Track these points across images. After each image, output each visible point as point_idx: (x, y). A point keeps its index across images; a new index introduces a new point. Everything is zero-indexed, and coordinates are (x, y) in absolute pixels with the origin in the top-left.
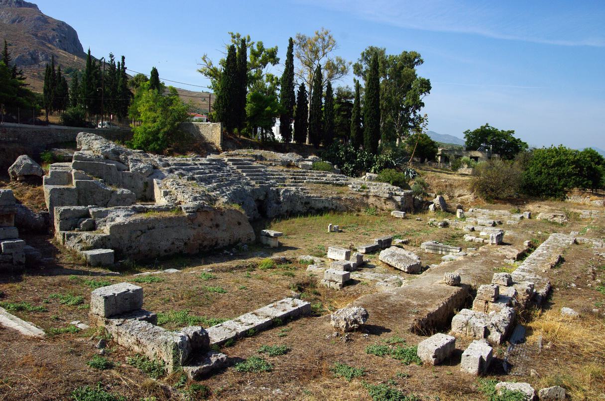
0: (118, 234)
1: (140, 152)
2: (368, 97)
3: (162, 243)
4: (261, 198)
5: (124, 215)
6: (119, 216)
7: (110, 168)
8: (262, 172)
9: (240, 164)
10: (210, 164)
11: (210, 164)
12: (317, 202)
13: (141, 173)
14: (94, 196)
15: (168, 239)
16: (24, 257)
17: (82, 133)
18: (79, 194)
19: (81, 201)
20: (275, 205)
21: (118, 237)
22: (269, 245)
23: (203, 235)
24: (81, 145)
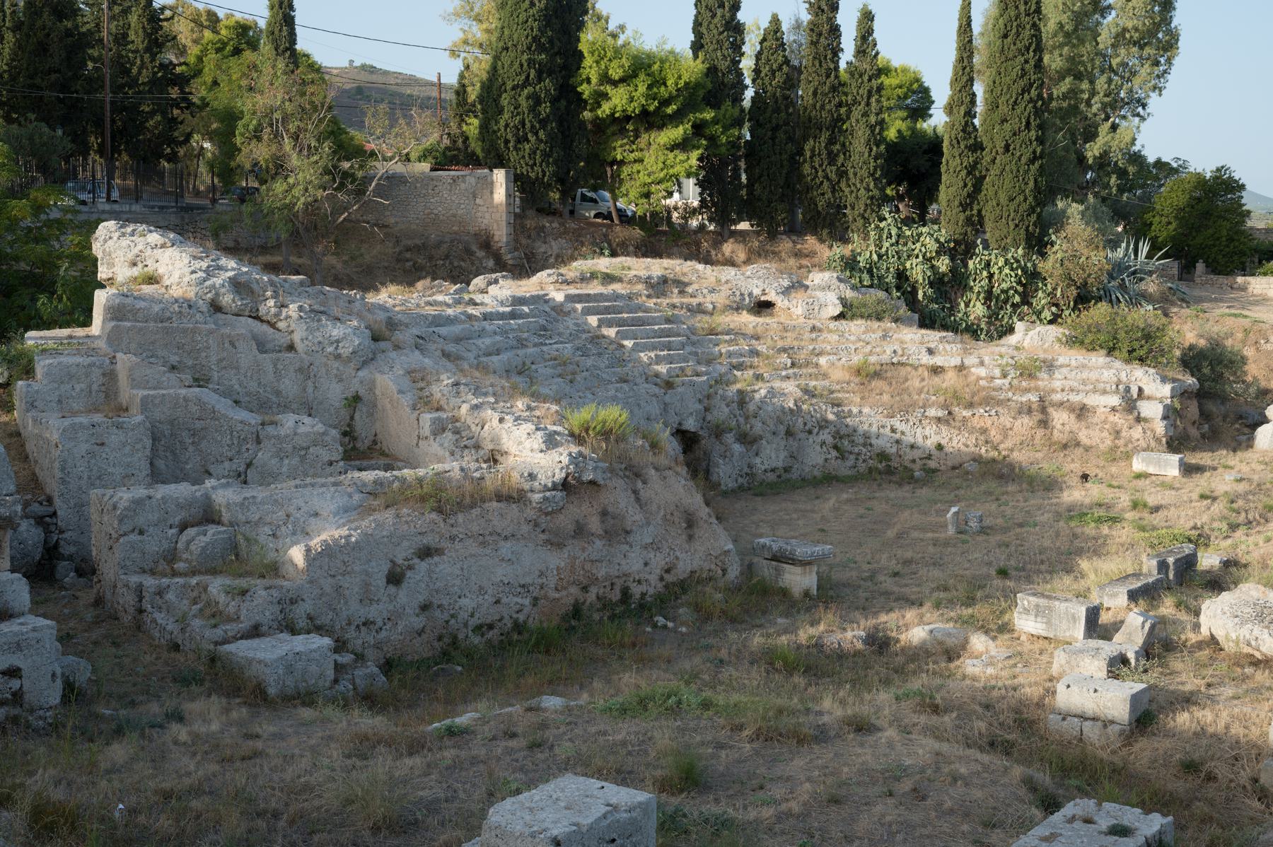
0: (330, 579)
1: (302, 283)
2: (1002, 55)
3: (464, 601)
4: (691, 424)
5: (333, 507)
6: (316, 514)
7: (232, 344)
9: (607, 310)
10: (513, 315)
11: (513, 315)
13: (338, 357)
14: (204, 444)
15: (481, 588)
16: (59, 682)
17: (111, 224)
18: (155, 439)
19: (160, 463)
20: (737, 448)
21: (328, 589)
22: (785, 593)
23: (588, 566)
24: (111, 265)
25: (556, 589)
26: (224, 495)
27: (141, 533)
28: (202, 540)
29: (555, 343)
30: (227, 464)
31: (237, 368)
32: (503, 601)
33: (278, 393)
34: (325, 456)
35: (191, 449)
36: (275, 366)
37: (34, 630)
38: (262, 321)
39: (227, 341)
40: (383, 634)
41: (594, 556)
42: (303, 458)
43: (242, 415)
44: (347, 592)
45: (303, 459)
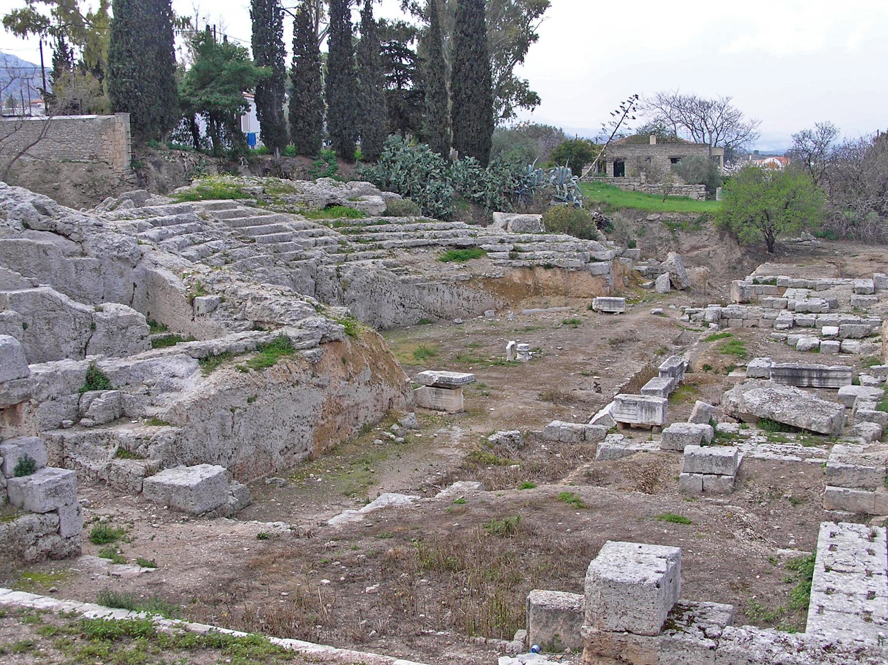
0: (202, 423)
8: (286, 230)
10: (178, 221)
11: (178, 221)
12: (425, 292)
14: (56, 329)
21: (200, 431)
25: (322, 419)
26: (107, 365)
27: (53, 399)
28: (101, 399)
29: (211, 240)
30: (73, 343)
31: (50, 270)
32: (295, 430)
33: (79, 288)
34: (137, 331)
35: (47, 333)
36: (76, 267)
37: (64, 478)
38: (59, 234)
39: (41, 250)
40: (233, 460)
41: (341, 394)
42: (124, 335)
43: (79, 306)
44: (211, 432)
45: (124, 335)
